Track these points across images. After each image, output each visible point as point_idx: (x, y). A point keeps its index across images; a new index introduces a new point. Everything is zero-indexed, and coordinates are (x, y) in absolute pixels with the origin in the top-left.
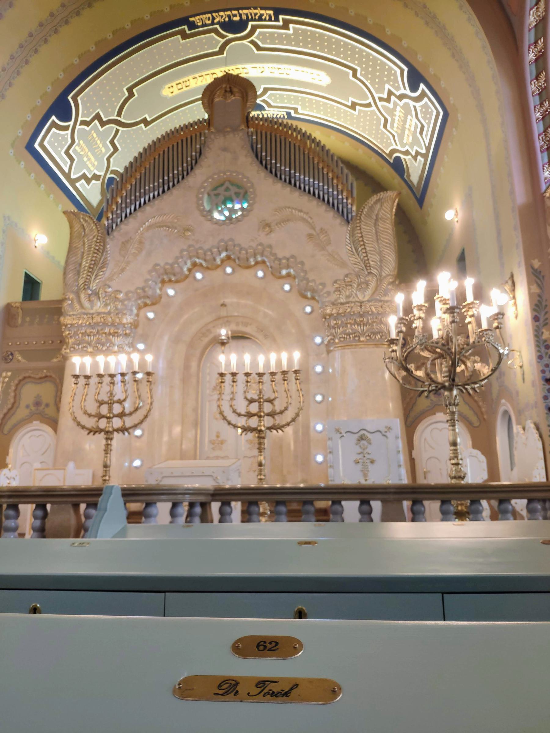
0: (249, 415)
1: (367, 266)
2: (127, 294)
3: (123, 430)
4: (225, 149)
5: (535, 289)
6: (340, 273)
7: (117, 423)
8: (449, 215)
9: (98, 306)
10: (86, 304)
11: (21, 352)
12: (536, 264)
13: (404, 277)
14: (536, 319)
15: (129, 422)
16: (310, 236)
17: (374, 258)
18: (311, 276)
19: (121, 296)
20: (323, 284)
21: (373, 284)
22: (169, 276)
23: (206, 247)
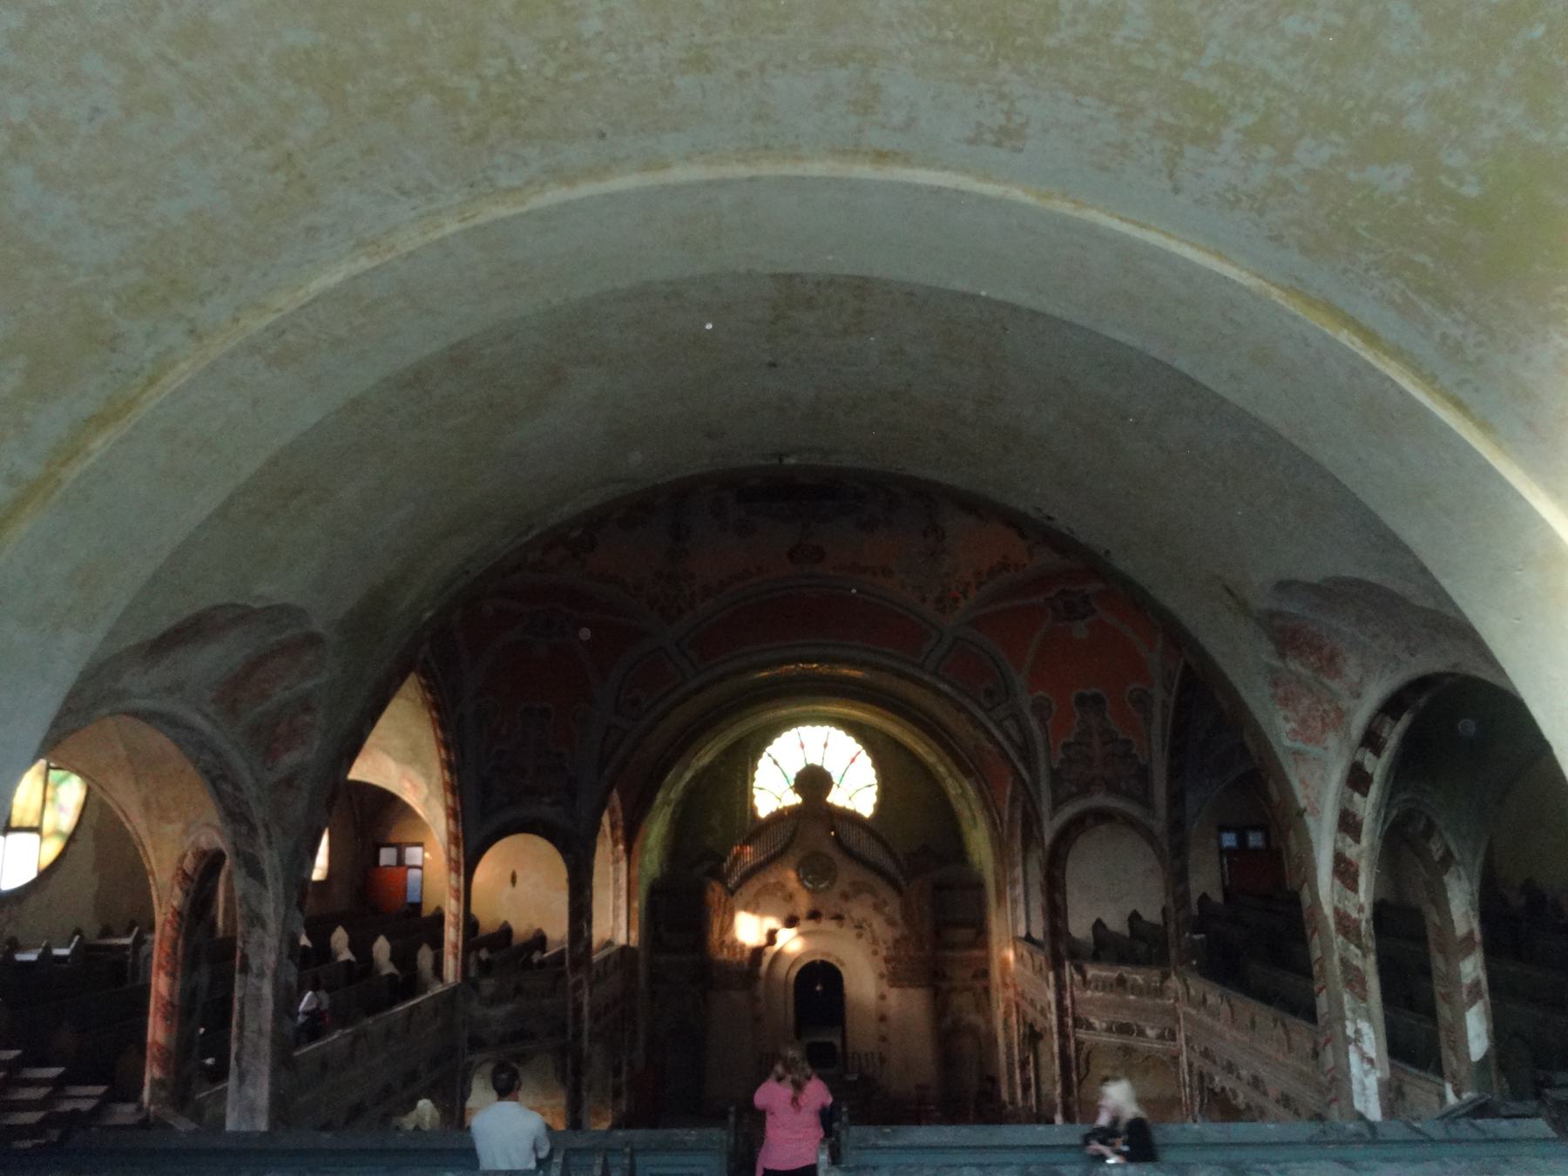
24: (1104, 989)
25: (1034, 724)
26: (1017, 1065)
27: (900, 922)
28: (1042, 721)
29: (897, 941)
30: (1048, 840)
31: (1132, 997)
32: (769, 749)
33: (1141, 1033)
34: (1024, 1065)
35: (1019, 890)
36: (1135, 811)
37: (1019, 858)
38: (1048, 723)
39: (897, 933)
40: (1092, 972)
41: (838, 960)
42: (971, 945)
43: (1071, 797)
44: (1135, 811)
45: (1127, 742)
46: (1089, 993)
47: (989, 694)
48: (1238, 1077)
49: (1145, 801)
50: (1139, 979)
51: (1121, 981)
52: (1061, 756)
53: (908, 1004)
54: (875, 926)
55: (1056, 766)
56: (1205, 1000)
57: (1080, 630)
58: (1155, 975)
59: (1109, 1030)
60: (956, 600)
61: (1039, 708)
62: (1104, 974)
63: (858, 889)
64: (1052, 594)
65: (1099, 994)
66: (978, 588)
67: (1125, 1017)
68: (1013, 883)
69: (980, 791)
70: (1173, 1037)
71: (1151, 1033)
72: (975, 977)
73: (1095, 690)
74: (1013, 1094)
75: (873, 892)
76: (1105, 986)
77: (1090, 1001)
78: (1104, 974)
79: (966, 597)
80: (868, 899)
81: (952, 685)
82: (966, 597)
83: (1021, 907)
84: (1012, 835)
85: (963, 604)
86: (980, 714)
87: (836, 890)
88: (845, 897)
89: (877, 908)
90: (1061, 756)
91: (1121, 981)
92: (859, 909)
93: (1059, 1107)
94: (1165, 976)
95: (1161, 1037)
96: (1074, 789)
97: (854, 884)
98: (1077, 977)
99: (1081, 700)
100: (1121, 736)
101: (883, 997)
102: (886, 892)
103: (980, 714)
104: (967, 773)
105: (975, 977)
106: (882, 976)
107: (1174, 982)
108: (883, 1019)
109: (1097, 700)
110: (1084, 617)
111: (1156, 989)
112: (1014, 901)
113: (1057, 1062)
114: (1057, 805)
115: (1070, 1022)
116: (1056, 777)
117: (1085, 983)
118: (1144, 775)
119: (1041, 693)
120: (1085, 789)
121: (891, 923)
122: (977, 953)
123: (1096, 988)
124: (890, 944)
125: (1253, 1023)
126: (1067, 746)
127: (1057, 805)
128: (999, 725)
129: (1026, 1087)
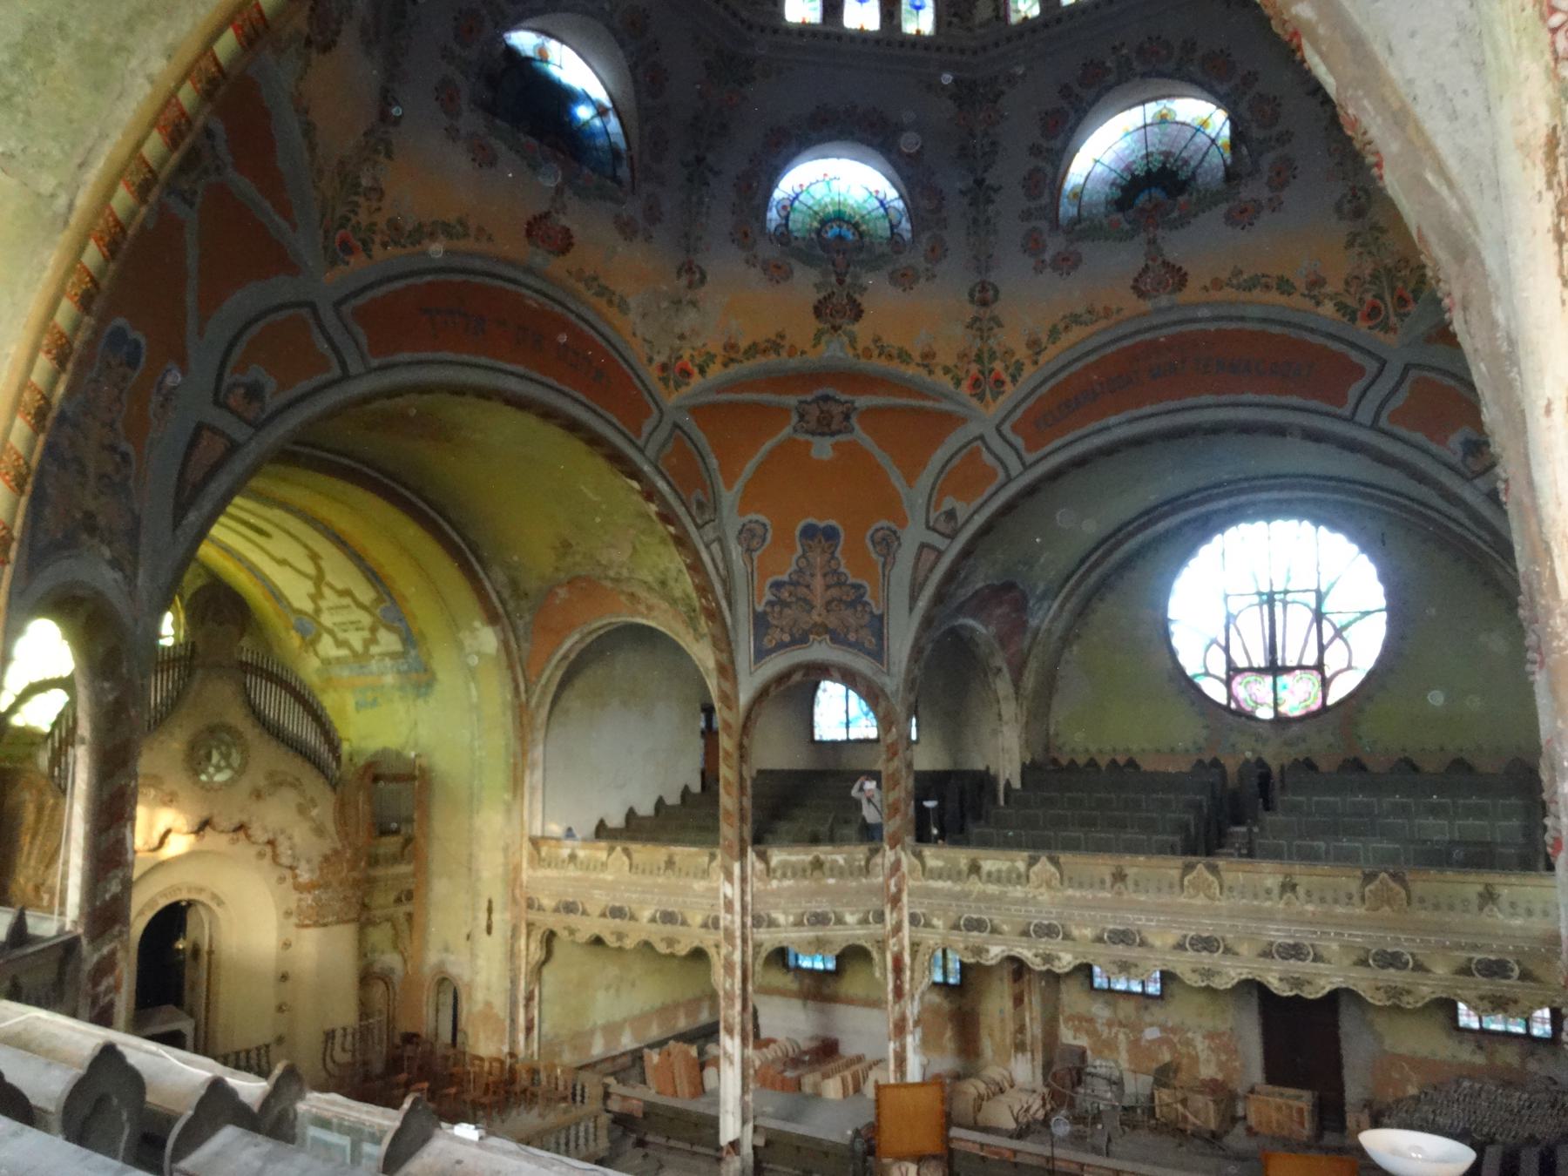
24: (794, 875)
25: (736, 552)
26: (522, 1002)
27: (331, 827)
28: (749, 551)
29: (326, 859)
30: (744, 697)
31: (831, 881)
33: (840, 921)
34: (529, 998)
35: (538, 774)
36: (862, 664)
37: (542, 733)
38: (755, 555)
39: (326, 846)
40: (777, 856)
41: (214, 897)
42: (396, 859)
43: (781, 646)
44: (862, 664)
45: (854, 586)
46: (775, 883)
47: (701, 505)
48: (1067, 937)
49: (878, 654)
50: (840, 859)
51: (818, 864)
52: (768, 596)
53: (323, 951)
54: (297, 839)
55: (760, 608)
56: (975, 868)
57: (823, 449)
58: (860, 853)
59: (798, 924)
60: (686, 373)
61: (748, 535)
62: (793, 858)
63: (277, 782)
64: (809, 398)
65: (787, 883)
66: (725, 365)
67: (822, 905)
68: (533, 767)
69: (505, 644)
70: (880, 917)
71: (850, 919)
72: (398, 900)
73: (833, 522)
74: (513, 1042)
75: (296, 784)
76: (797, 872)
77: (777, 893)
78: (793, 858)
79: (702, 371)
80: (290, 796)
81: (669, 483)
82: (702, 371)
83: (539, 795)
84: (538, 706)
85: (696, 380)
86: (692, 529)
87: (245, 784)
88: (258, 795)
89: (302, 810)
90: (768, 596)
91: (818, 864)
92: (275, 814)
93: (737, 1029)
94: (874, 852)
95: (864, 921)
96: (786, 638)
97: (271, 775)
98: (760, 866)
99: (809, 532)
100: (851, 580)
101: (287, 945)
102: (315, 786)
103: (692, 529)
104: (493, 618)
105: (398, 900)
106: (288, 914)
107: (889, 855)
108: (284, 977)
109: (831, 534)
110: (833, 434)
111: (860, 868)
112: (533, 789)
113: (738, 973)
114: (761, 654)
115: (749, 920)
116: (761, 623)
117: (769, 871)
118: (878, 625)
119: (754, 517)
120: (800, 640)
121: (319, 831)
122: (404, 869)
123: (784, 876)
124: (317, 860)
125: (1119, 877)
126: (777, 585)
127: (761, 654)
128: (707, 546)
129: (529, 1029)
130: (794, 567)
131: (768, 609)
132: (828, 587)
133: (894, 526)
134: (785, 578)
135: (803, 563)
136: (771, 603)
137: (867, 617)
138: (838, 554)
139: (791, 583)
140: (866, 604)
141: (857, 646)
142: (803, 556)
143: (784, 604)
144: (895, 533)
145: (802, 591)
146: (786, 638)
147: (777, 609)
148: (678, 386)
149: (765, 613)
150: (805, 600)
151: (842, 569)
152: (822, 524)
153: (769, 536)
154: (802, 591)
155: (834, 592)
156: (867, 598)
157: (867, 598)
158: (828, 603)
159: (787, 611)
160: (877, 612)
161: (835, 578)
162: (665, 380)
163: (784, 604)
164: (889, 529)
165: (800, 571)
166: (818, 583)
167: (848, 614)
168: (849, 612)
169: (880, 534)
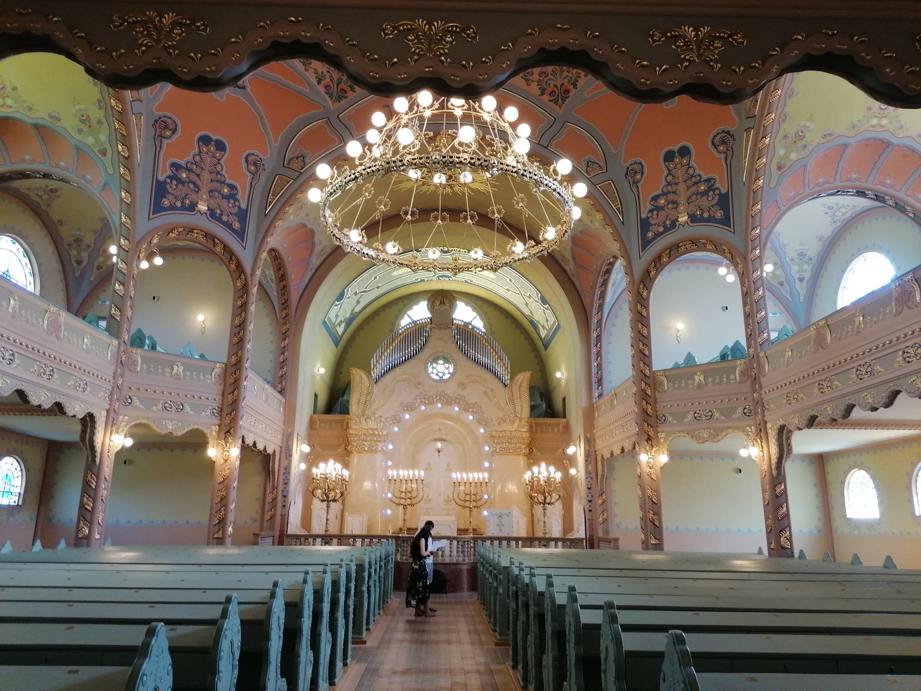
0: (466, 501)
1: (515, 413)
2: (386, 418)
3: (412, 505)
4: (441, 339)
5: (587, 448)
6: (501, 414)
7: (409, 501)
8: (558, 375)
9: (372, 424)
10: (364, 422)
11: (319, 445)
12: (589, 436)
13: (529, 468)
14: (586, 461)
15: (414, 501)
16: (485, 393)
17: (518, 409)
18: (485, 415)
19: (383, 419)
20: (492, 420)
21: (517, 422)
22: (410, 408)
23: (430, 394)
32: (409, 313)
52: (649, 207)
55: (644, 216)
60: (567, 91)
82: (575, 86)
96: (661, 229)
100: (704, 177)
109: (684, 152)
114: (645, 243)
127: (645, 243)
130: (664, 183)
131: (650, 215)
132: (688, 188)
133: (729, 128)
134: (659, 192)
135: (669, 178)
136: (651, 211)
137: (717, 198)
138: (692, 163)
139: (664, 194)
140: (718, 189)
141: (711, 219)
142: (670, 173)
143: (659, 208)
144: (728, 132)
145: (671, 197)
146: (661, 229)
147: (655, 212)
148: (563, 101)
149: (648, 218)
150: (673, 202)
151: (698, 172)
152: (676, 148)
153: (645, 170)
154: (671, 197)
155: (693, 189)
156: (717, 185)
157: (717, 185)
158: (690, 198)
159: (661, 213)
160: (724, 191)
161: (693, 180)
162: (556, 101)
163: (659, 208)
164: (723, 132)
165: (669, 184)
166: (681, 188)
167: (704, 202)
168: (705, 197)
169: (719, 137)
